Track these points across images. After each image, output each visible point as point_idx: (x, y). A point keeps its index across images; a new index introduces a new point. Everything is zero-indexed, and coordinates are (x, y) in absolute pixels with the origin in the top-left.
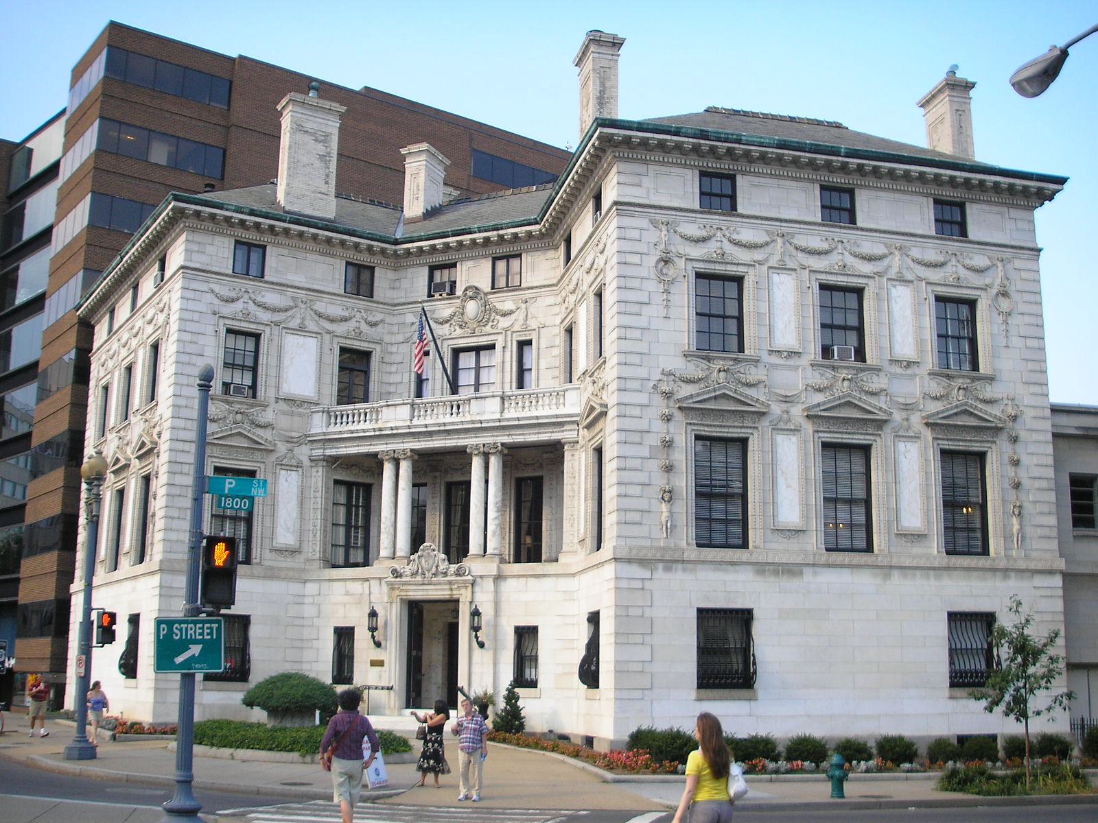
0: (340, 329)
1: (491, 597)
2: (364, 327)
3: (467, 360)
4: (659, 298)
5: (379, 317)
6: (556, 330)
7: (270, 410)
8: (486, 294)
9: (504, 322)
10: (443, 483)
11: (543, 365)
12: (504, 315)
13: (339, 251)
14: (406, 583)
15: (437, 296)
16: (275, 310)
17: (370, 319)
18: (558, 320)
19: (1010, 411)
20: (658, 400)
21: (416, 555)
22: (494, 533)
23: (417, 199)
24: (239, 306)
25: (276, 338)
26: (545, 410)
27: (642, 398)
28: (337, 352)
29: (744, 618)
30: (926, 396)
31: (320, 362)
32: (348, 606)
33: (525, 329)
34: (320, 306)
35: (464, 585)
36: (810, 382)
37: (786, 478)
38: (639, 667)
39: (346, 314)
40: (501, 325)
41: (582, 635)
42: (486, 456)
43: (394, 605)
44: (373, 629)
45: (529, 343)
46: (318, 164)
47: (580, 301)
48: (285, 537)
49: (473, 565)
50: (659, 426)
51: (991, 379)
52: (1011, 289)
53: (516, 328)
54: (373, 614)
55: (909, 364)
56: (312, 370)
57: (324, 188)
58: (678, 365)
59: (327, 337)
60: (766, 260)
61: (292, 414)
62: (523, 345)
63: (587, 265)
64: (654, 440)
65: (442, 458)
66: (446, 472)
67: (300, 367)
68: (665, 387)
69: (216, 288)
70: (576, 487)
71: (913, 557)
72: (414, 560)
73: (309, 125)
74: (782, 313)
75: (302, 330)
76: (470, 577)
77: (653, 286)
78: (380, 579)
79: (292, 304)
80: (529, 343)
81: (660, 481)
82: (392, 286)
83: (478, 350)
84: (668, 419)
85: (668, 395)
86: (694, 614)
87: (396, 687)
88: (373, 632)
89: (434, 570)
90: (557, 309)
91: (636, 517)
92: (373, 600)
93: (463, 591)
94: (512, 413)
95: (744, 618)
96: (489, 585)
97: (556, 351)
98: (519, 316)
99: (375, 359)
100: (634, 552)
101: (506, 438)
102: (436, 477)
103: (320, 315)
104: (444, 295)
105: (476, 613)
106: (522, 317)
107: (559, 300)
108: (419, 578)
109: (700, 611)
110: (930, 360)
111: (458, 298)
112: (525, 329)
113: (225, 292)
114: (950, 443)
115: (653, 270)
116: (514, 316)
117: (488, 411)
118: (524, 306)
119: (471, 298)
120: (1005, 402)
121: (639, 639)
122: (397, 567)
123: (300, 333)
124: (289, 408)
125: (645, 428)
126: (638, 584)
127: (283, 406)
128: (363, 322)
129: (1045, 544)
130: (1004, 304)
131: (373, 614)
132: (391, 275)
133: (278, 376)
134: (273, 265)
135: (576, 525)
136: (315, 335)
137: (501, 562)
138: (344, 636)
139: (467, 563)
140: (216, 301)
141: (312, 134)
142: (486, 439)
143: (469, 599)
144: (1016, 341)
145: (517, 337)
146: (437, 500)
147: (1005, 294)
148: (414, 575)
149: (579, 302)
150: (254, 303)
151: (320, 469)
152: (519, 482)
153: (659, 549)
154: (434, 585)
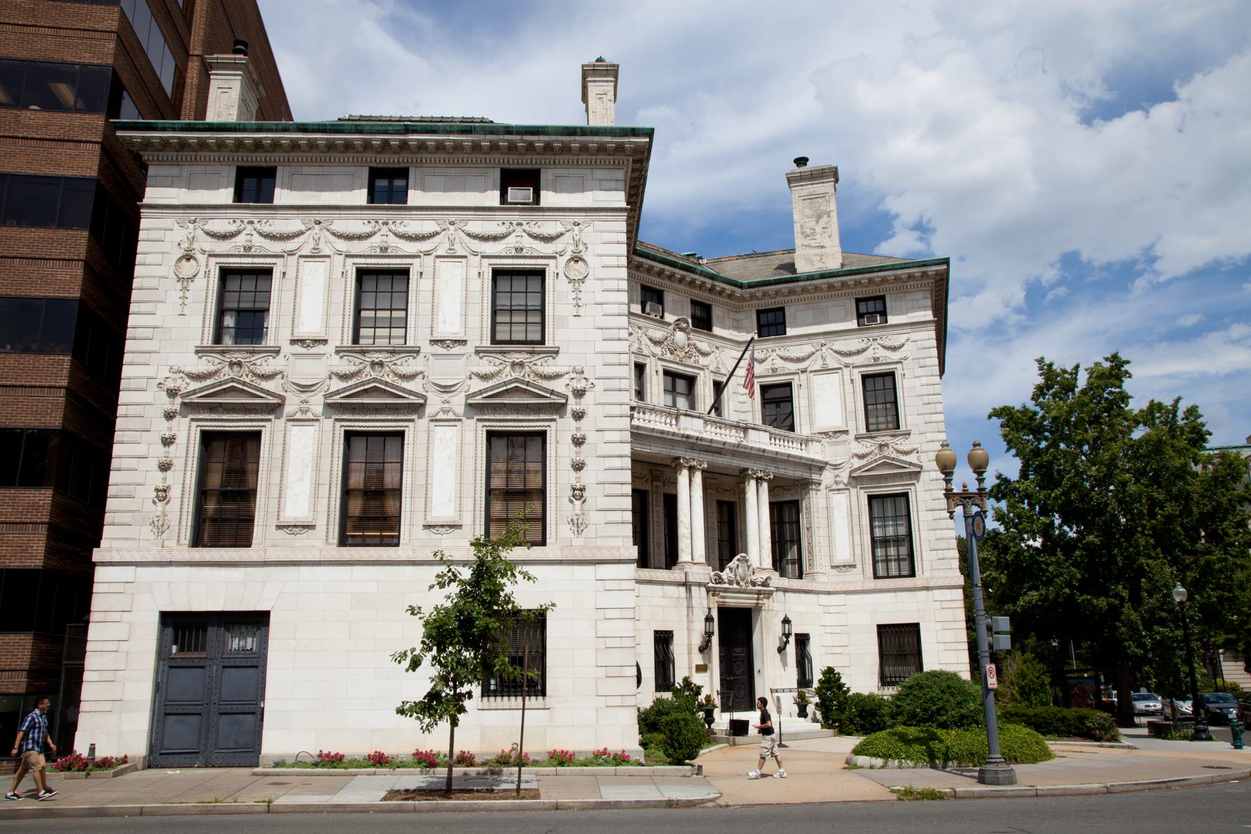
9: (703, 361)
12: (705, 354)
14: (726, 590)
111: (669, 324)
119: (682, 330)
152: (720, 504)
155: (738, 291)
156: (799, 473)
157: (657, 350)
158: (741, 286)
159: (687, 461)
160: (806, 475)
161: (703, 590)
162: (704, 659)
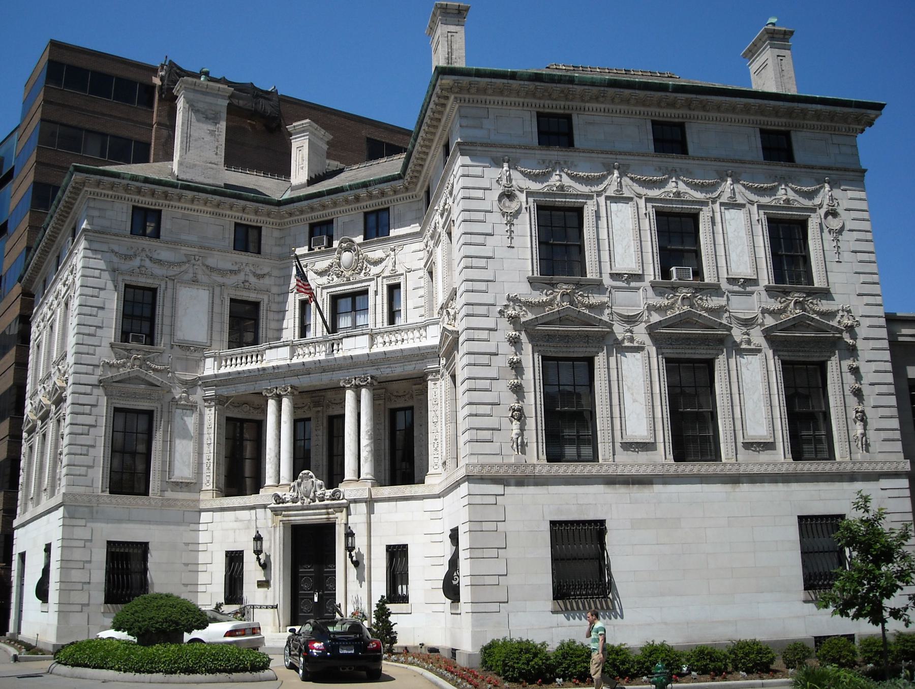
0: (231, 280)
1: (363, 518)
2: (252, 280)
3: (345, 304)
4: (502, 229)
5: (266, 270)
6: (421, 273)
7: (166, 355)
8: (359, 245)
9: (375, 270)
11: (410, 305)
12: (376, 263)
14: (288, 509)
15: (316, 250)
17: (259, 272)
18: (423, 263)
19: (847, 321)
20: (504, 323)
21: (295, 483)
22: (366, 459)
23: (302, 168)
24: (136, 262)
25: (170, 291)
26: (412, 342)
27: (489, 323)
28: (227, 303)
29: (597, 529)
30: (764, 311)
31: (212, 312)
32: (237, 531)
33: (394, 275)
34: (211, 262)
35: (339, 508)
36: (650, 302)
37: (632, 395)
38: (494, 580)
39: (235, 268)
40: (372, 273)
41: (447, 550)
42: (357, 389)
43: (278, 529)
44: (258, 552)
45: (398, 286)
46: (208, 138)
48: (182, 471)
49: (348, 490)
50: (507, 350)
51: (825, 294)
52: (840, 210)
53: (385, 274)
54: (258, 538)
55: (748, 282)
56: (204, 319)
57: (215, 159)
58: (524, 291)
60: (605, 190)
62: (394, 289)
63: (441, 208)
64: (502, 362)
66: (328, 406)
67: (193, 314)
68: (511, 312)
69: (116, 248)
70: (438, 413)
71: (761, 464)
73: (200, 106)
74: (621, 236)
76: (344, 501)
77: (496, 217)
78: (265, 507)
79: (185, 260)
80: (398, 286)
81: (510, 400)
83: (353, 295)
84: (515, 342)
85: (514, 320)
86: (547, 526)
87: (280, 607)
88: (258, 555)
89: (312, 495)
90: (421, 254)
91: (486, 435)
92: (259, 526)
93: (338, 515)
94: (379, 348)
95: (597, 529)
96: (363, 507)
97: (421, 292)
98: (388, 263)
99: (263, 308)
100: (487, 468)
102: (318, 411)
103: (212, 269)
104: (323, 249)
105: (349, 534)
106: (390, 265)
107: (422, 245)
108: (299, 504)
109: (553, 523)
110: (766, 278)
111: (335, 249)
112: (394, 275)
113: (123, 251)
114: (790, 354)
115: (496, 203)
116: (384, 264)
117: (355, 347)
118: (392, 253)
120: (841, 313)
121: (494, 553)
122: (280, 494)
125: (494, 350)
126: (492, 500)
127: (178, 351)
128: (251, 275)
129: (889, 447)
130: (835, 224)
131: (258, 538)
132: (276, 234)
133: (172, 325)
134: (168, 227)
135: (439, 449)
137: (373, 486)
138: (234, 559)
139: (342, 487)
140: (115, 259)
141: (203, 113)
143: (344, 521)
144: (846, 256)
145: (386, 282)
146: (320, 433)
147: (833, 213)
148: (294, 501)
149: (437, 244)
150: (152, 261)
151: (213, 409)
152: (393, 413)
153: (509, 465)
156: (410, 369)
157: (324, 280)
158: (399, 177)
159: (271, 391)
161: (268, 511)
162: (265, 575)
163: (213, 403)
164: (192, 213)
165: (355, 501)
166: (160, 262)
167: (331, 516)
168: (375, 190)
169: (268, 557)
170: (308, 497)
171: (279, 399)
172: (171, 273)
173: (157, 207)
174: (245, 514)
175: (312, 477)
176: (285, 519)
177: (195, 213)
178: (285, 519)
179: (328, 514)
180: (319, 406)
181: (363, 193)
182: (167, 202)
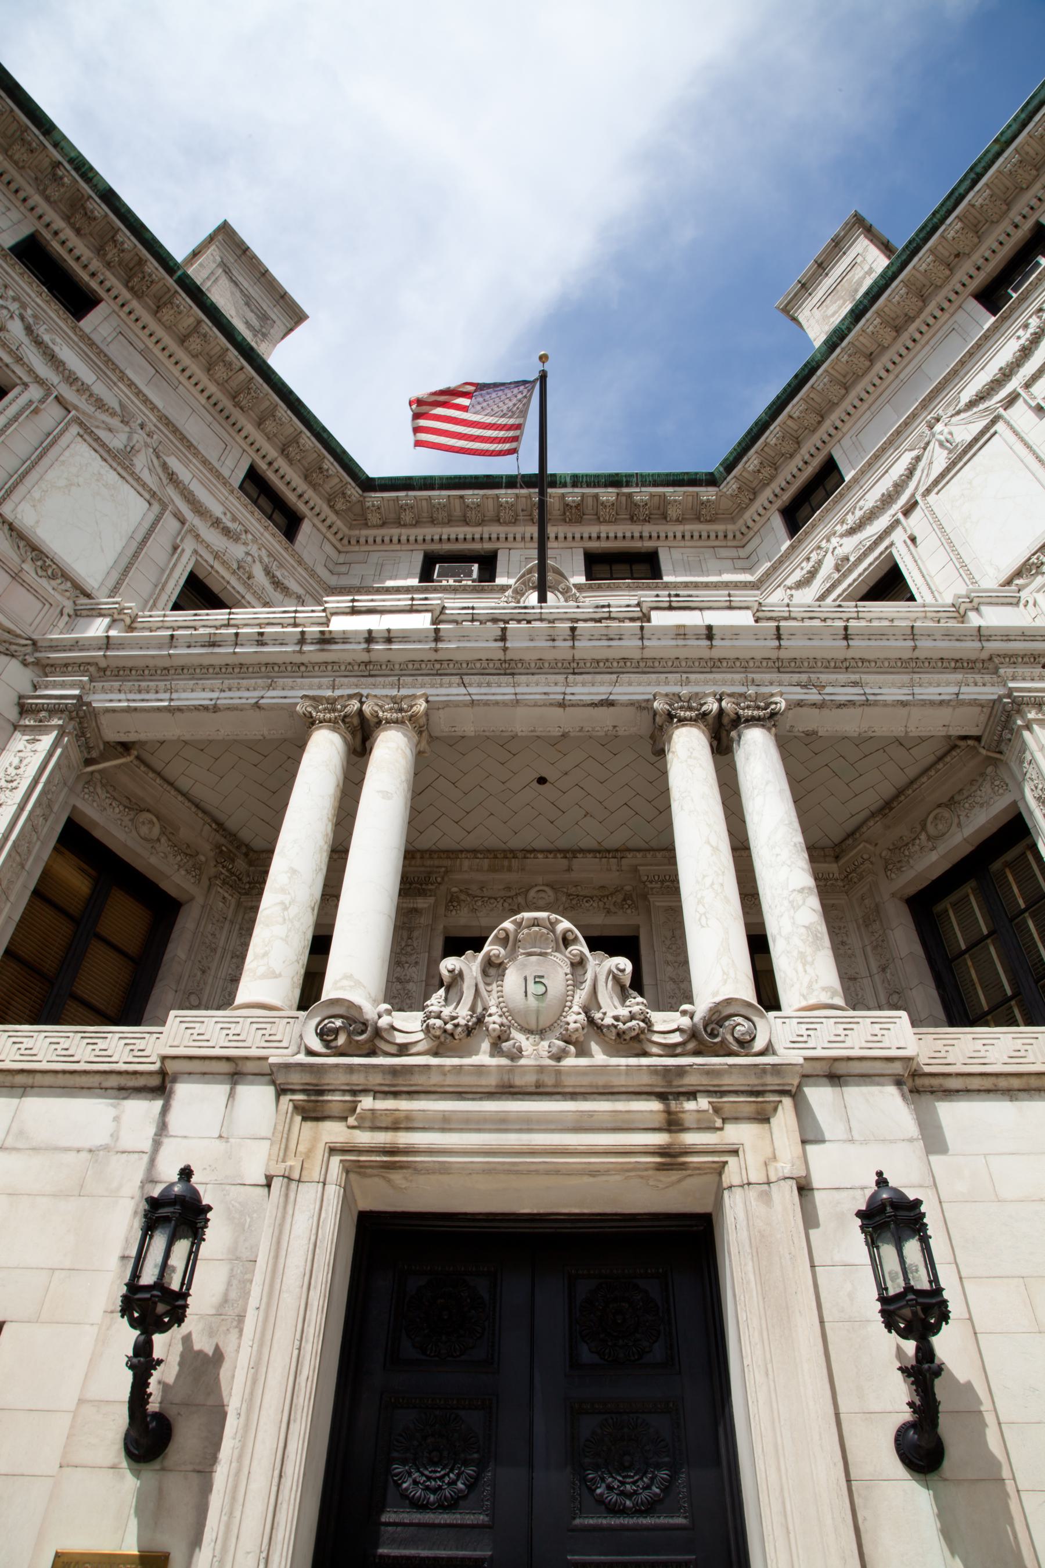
8: (579, 587)
10: (440, 928)
13: (249, 428)
16: (71, 379)
43: (307, 1195)
44: (152, 1306)
47: (936, 482)
54: (177, 1214)
59: (170, 524)
61: (16, 576)
65: (449, 863)
66: (453, 901)
72: (458, 977)
75: (120, 460)
78: (235, 1071)
82: (331, 567)
89: (575, 1019)
93: (735, 1133)
101: (798, 689)
108: (483, 1057)
123: (115, 465)
124: (17, 559)
136: (147, 496)
142: (713, 693)
151: (47, 741)
154: (573, 1096)
155: (707, 493)
158: (711, 480)
160: (989, 692)
161: (257, 1100)
163: (56, 721)
164: (169, 364)
165: (835, 1073)
166: (52, 358)
167: (690, 1139)
168: (641, 494)
169: (203, 1367)
170: (541, 1033)
171: (360, 738)
172: (69, 394)
173: (94, 284)
174: (90, 1117)
175: (566, 941)
176: (365, 1138)
177: (176, 371)
178: (365, 1138)
179: (673, 1124)
180: (422, 893)
181: (608, 495)
182: (126, 295)
